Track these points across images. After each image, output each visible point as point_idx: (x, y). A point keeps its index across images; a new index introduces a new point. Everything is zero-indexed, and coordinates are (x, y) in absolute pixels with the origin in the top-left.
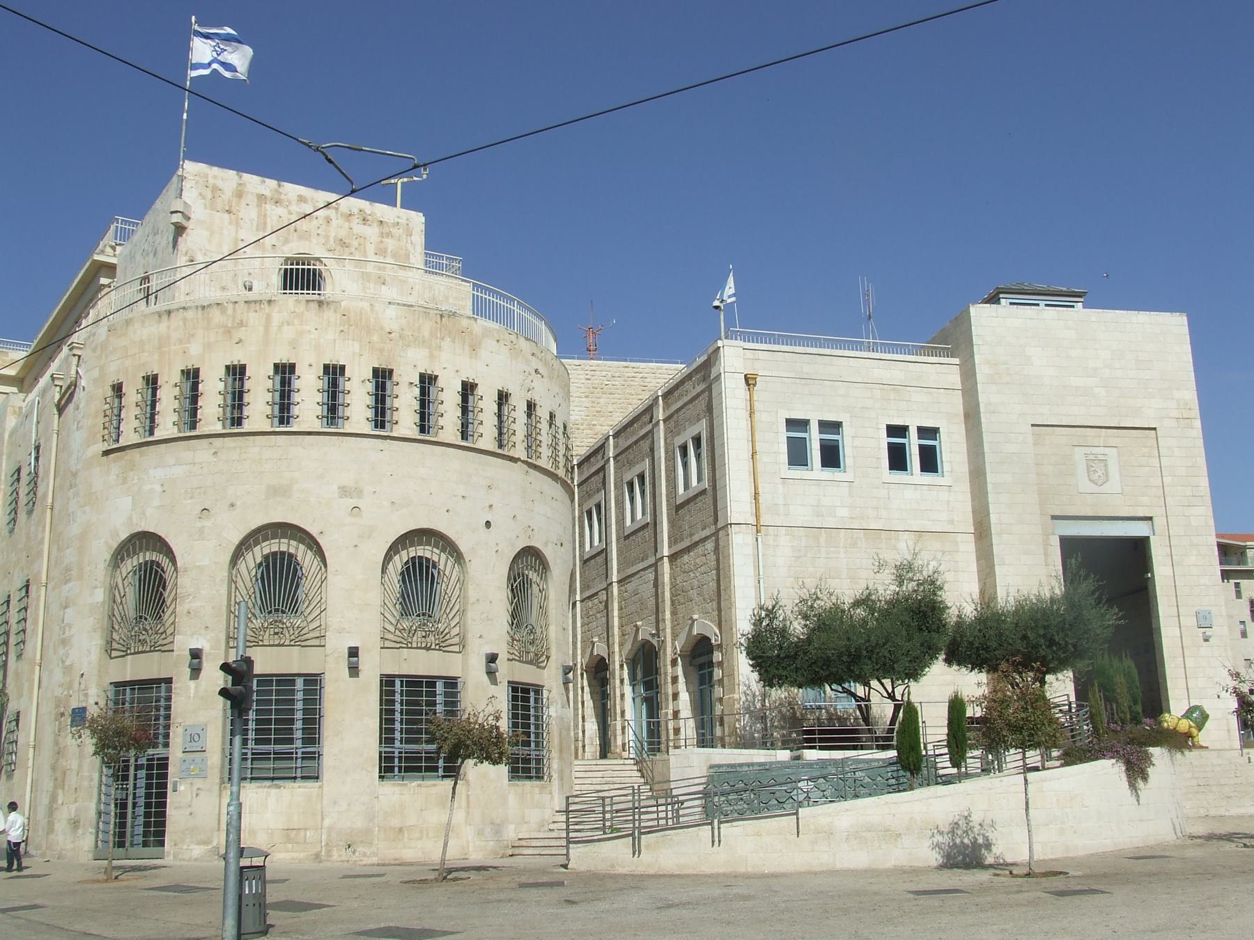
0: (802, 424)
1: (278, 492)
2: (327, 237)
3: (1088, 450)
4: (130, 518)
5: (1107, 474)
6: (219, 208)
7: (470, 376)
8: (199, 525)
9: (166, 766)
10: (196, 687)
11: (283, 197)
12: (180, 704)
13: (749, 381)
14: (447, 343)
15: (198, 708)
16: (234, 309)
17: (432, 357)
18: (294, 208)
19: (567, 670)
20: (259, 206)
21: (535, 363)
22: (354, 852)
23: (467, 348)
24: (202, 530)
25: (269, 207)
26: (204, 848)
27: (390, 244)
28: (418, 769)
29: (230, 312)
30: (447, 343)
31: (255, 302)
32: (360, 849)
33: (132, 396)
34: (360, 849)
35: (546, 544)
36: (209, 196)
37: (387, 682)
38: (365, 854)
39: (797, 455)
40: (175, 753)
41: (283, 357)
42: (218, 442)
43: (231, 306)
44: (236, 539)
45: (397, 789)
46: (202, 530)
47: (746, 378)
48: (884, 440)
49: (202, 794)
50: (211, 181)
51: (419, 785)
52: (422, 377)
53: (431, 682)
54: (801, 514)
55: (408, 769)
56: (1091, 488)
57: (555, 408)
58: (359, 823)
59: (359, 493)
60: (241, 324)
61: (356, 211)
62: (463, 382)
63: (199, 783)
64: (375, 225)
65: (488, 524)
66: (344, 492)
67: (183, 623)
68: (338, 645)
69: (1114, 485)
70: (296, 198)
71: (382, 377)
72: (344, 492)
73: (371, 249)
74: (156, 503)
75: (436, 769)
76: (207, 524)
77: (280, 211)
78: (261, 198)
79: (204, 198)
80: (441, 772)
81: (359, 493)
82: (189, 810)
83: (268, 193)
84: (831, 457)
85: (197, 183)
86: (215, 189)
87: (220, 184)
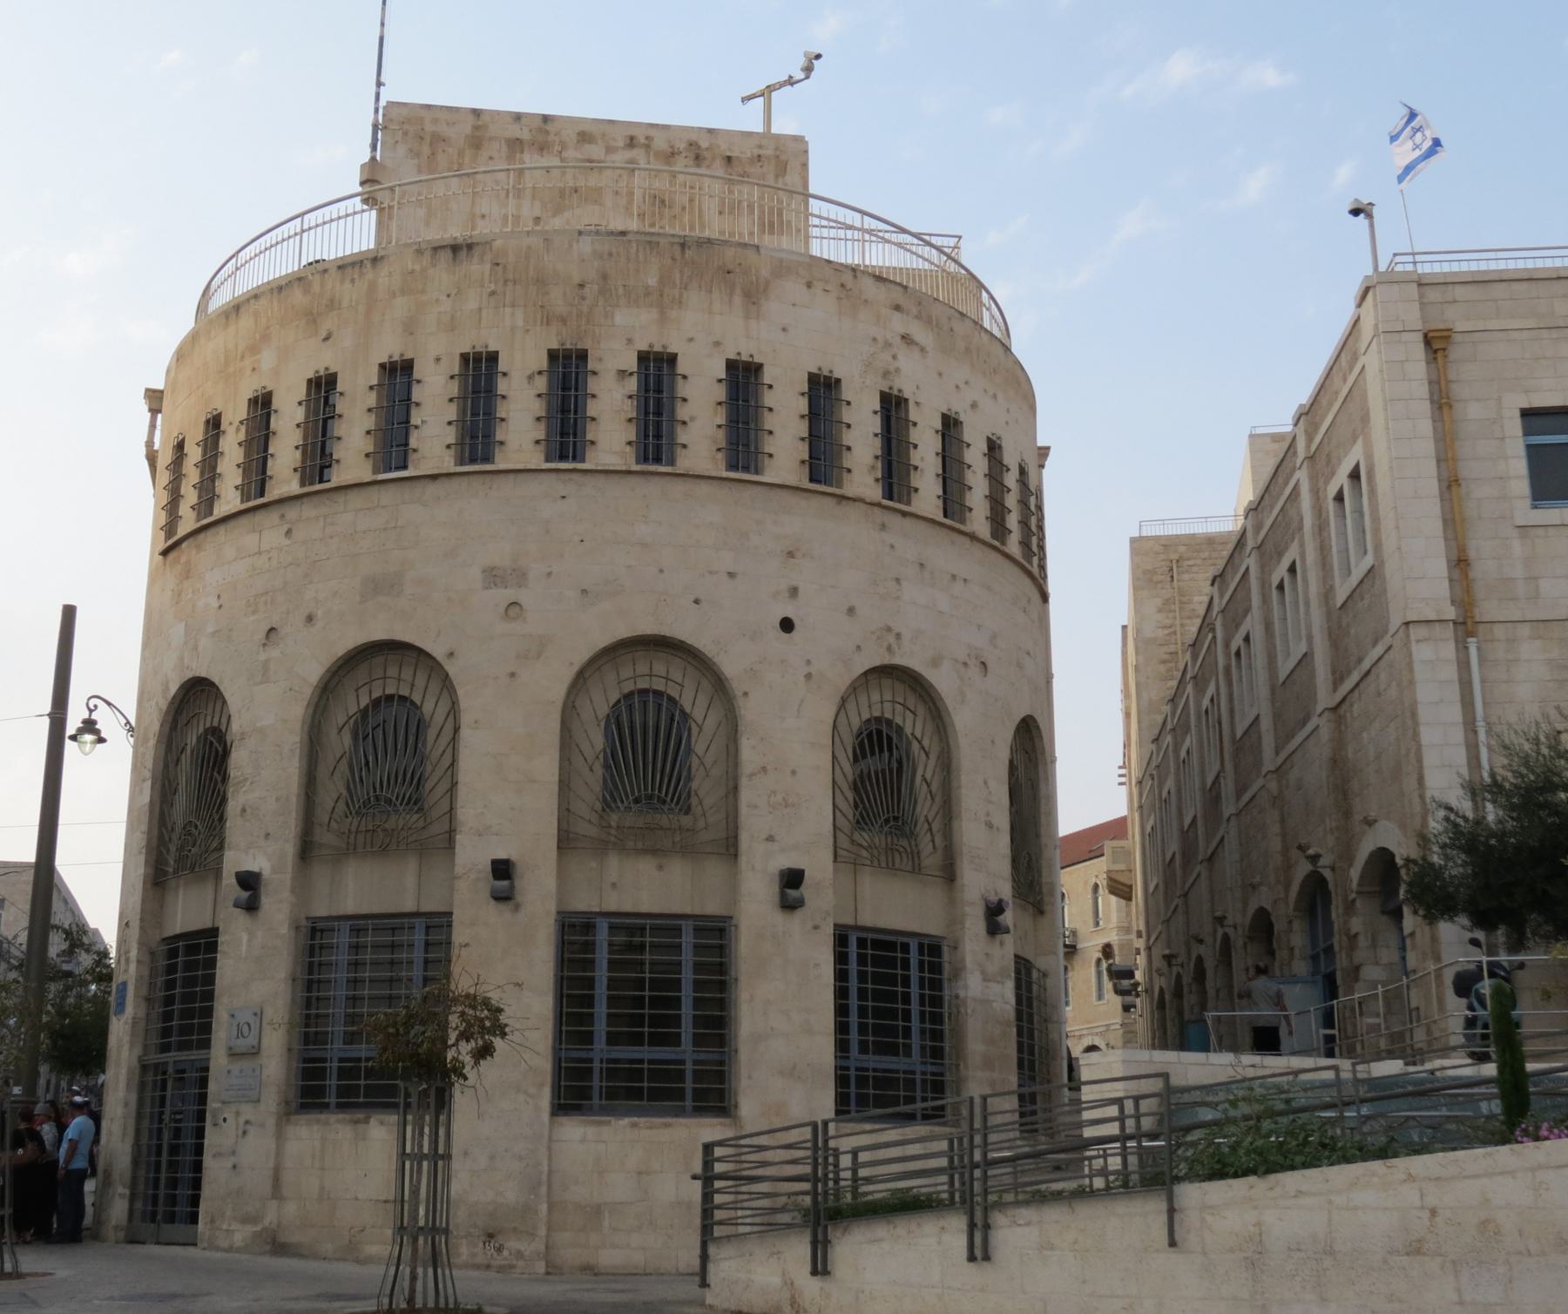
1: (380, 587)
4: (181, 659)
7: (745, 349)
8: (263, 657)
9: (204, 1082)
10: (250, 941)
11: (551, 138)
12: (231, 969)
14: (694, 297)
15: (255, 979)
16: (322, 284)
17: (663, 319)
18: (570, 153)
19: (994, 911)
20: (510, 158)
21: (899, 324)
22: (499, 1250)
23: (738, 299)
24: (266, 665)
25: (530, 159)
26: (250, 1229)
27: (748, 193)
29: (316, 288)
30: (694, 297)
31: (353, 264)
32: (513, 1244)
33: (194, 454)
34: (513, 1244)
35: (936, 662)
36: (426, 150)
37: (575, 934)
38: (519, 1255)
40: (218, 1057)
41: (389, 347)
42: (292, 512)
43: (317, 277)
44: (313, 671)
45: (591, 1131)
46: (266, 665)
49: (252, 1130)
50: (429, 127)
51: (634, 1125)
52: (643, 357)
53: (668, 925)
55: (612, 1094)
57: (959, 407)
58: (511, 1195)
59: (519, 576)
60: (333, 304)
61: (682, 146)
62: (731, 365)
63: (248, 1111)
64: (718, 163)
66: (493, 577)
67: (235, 826)
68: (473, 855)
70: (574, 137)
71: (568, 373)
72: (493, 577)
74: (210, 629)
75: (679, 1095)
76: (274, 653)
78: (515, 145)
79: (418, 155)
81: (519, 576)
82: (233, 1160)
83: (525, 135)
85: (406, 133)
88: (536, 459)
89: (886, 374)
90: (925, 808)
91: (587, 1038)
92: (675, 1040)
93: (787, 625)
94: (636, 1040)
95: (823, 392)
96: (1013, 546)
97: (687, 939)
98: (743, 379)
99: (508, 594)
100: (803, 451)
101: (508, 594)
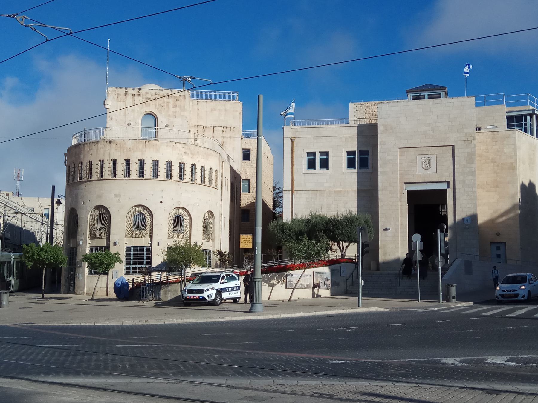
0: (314, 154)
2: (156, 104)
3: (423, 156)
5: (430, 166)
6: (119, 100)
13: (292, 140)
21: (183, 150)
27: (178, 103)
28: (136, 272)
35: (188, 206)
36: (116, 97)
39: (311, 165)
47: (291, 139)
48: (346, 157)
54: (310, 186)
56: (424, 171)
59: (120, 196)
65: (161, 202)
66: (116, 196)
69: (433, 169)
72: (116, 196)
73: (171, 106)
77: (140, 98)
78: (133, 95)
80: (131, 273)
84: (325, 164)
86: (118, 94)
87: (119, 92)
88: (123, 177)
89: (181, 159)
90: (187, 228)
91: (130, 264)
92: (143, 264)
93: (161, 202)
94: (137, 264)
95: (169, 165)
96: (207, 183)
97: (145, 250)
98: (156, 163)
99: (118, 198)
100: (165, 174)
101: (118, 198)
